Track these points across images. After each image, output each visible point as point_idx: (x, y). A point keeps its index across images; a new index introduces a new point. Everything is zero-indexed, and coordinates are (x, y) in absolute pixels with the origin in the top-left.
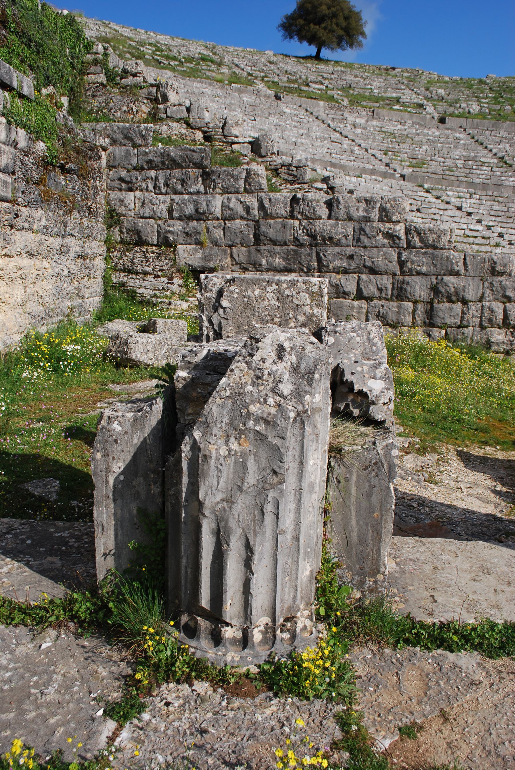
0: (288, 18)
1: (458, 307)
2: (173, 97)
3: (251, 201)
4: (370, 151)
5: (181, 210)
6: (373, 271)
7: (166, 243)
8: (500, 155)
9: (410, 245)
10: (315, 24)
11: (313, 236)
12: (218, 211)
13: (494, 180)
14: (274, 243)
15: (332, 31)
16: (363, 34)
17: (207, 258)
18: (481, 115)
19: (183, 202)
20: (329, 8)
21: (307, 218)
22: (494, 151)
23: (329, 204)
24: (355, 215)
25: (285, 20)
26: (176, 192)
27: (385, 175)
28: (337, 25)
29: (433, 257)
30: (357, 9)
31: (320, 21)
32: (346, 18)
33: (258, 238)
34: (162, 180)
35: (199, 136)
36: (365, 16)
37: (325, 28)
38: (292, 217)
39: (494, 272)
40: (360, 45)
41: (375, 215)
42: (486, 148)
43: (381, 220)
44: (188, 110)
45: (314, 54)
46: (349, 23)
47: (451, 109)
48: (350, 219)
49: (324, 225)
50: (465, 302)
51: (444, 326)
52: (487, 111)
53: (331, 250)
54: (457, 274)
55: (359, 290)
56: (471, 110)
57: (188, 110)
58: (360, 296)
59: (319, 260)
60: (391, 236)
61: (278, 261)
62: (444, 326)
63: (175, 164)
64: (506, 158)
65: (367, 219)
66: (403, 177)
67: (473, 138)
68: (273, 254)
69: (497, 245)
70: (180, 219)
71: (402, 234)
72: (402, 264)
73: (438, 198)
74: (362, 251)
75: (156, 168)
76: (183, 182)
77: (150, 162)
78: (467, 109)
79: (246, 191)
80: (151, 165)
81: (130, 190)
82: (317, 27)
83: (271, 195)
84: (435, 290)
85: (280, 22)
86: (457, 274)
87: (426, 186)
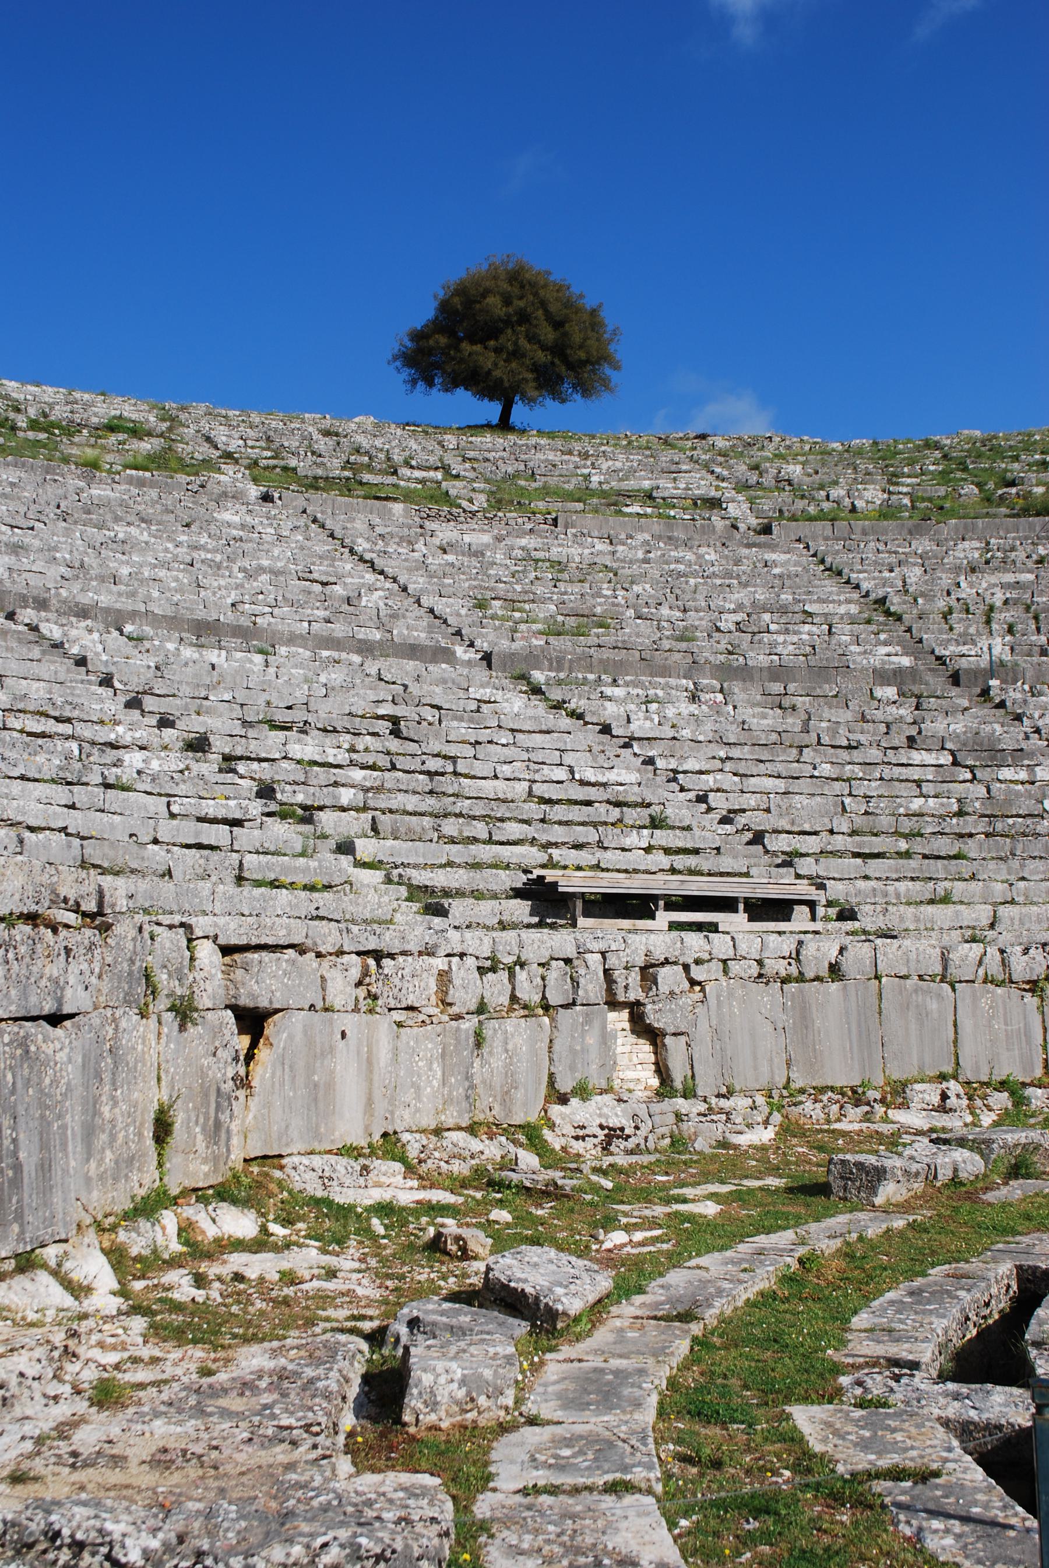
0: (418, 336)
10: (473, 342)
15: (516, 354)
18: (888, 512)
20: (507, 301)
22: (865, 586)
25: (409, 344)
28: (532, 338)
30: (589, 303)
31: (487, 332)
32: (558, 325)
36: (610, 318)
37: (497, 351)
42: (848, 582)
45: (495, 421)
46: (565, 334)
47: (800, 504)
52: (906, 501)
56: (860, 504)
67: (822, 561)
69: (656, 823)
73: (558, 706)
78: (847, 502)
82: (478, 348)
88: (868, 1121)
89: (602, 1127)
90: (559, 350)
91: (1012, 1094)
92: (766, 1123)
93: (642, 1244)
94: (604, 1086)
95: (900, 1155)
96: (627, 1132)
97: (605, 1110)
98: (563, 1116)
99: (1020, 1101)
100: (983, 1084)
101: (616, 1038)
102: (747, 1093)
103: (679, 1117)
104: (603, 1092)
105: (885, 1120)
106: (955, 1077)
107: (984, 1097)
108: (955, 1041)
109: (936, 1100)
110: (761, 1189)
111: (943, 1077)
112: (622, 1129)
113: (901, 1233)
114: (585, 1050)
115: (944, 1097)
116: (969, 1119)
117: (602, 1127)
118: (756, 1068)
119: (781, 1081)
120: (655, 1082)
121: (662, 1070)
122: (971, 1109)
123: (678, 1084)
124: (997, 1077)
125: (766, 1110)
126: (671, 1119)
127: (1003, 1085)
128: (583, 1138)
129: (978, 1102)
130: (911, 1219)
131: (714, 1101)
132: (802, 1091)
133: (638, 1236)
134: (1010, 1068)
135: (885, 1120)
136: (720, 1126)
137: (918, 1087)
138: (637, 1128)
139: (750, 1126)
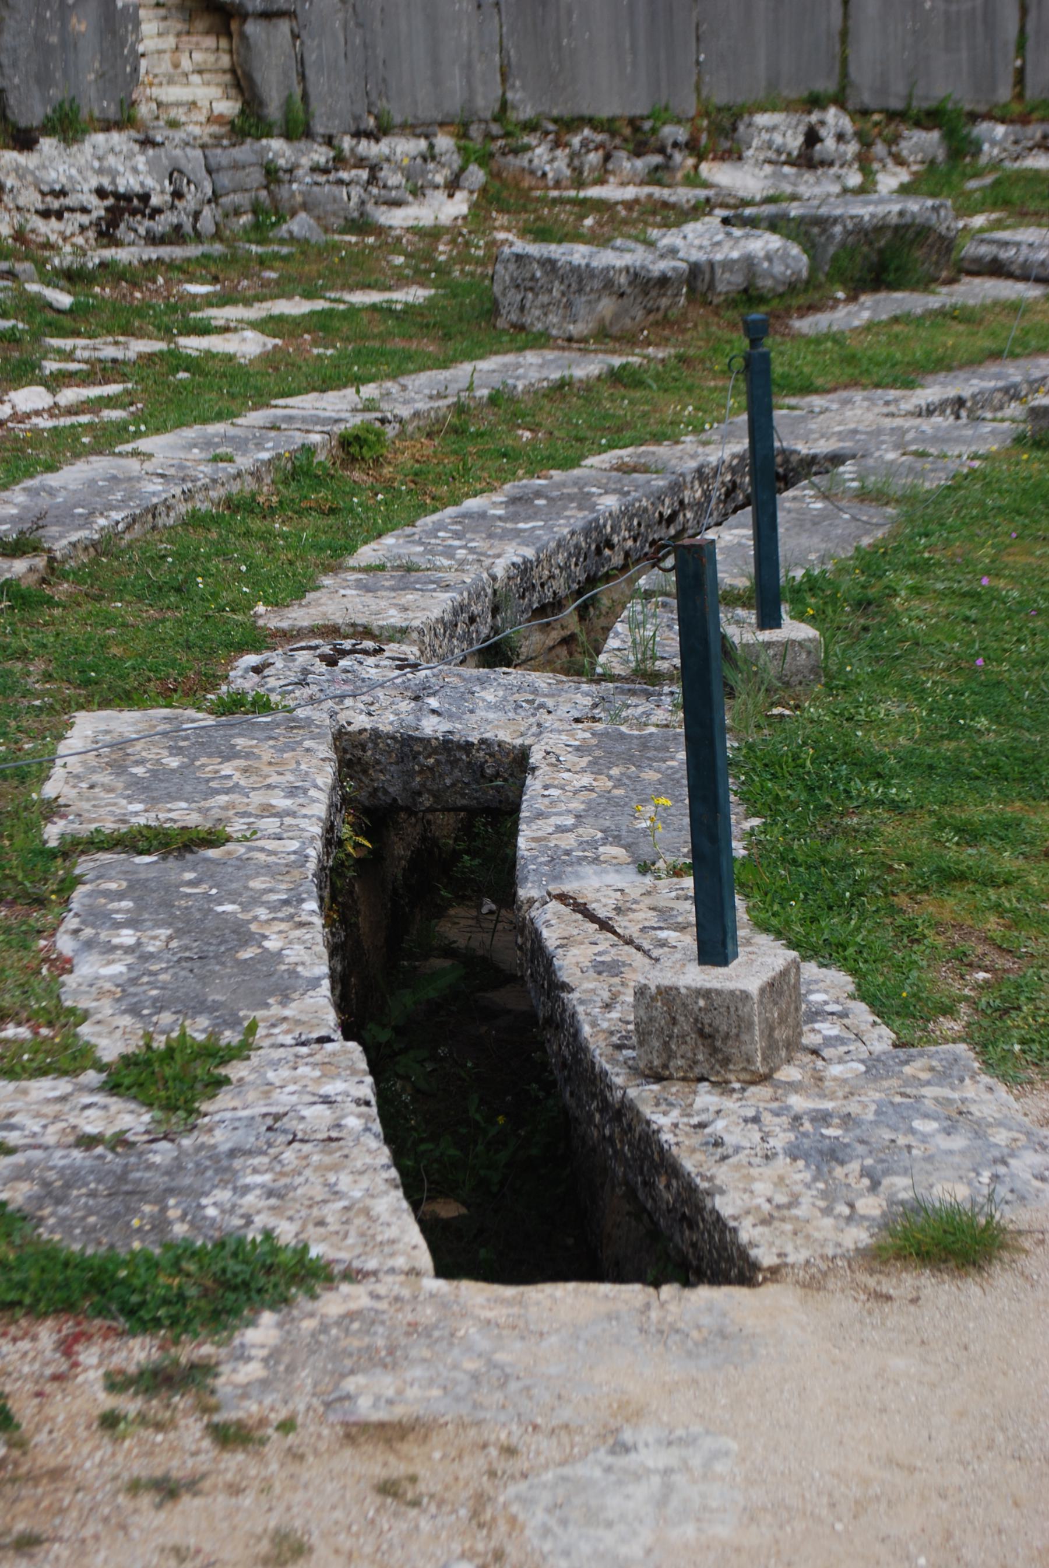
88: (659, 183)
89: (101, 193)
91: (950, 135)
92: (452, 186)
93: (72, 411)
94: (112, 111)
95: (650, 244)
96: (155, 201)
97: (111, 161)
98: (20, 172)
99: (961, 149)
100: (892, 116)
101: (137, 24)
102: (411, 129)
103: (272, 174)
104: (107, 126)
105: (693, 180)
106: (840, 101)
107: (893, 140)
108: (844, 34)
109: (795, 142)
110: (374, 308)
111: (815, 102)
112: (145, 197)
113: (588, 389)
114: (69, 43)
115: (812, 137)
116: (855, 179)
117: (101, 193)
118: (436, 81)
119: (485, 103)
120: (228, 107)
121: (242, 82)
122: (864, 162)
123: (274, 110)
124: (919, 105)
125: (456, 161)
126: (256, 177)
127: (931, 118)
128: (59, 215)
129: (879, 149)
130: (617, 361)
131: (347, 143)
132: (531, 127)
133: (69, 396)
134: (947, 85)
135: (693, 180)
136: (356, 192)
137: (762, 119)
138: (178, 195)
139: (418, 192)
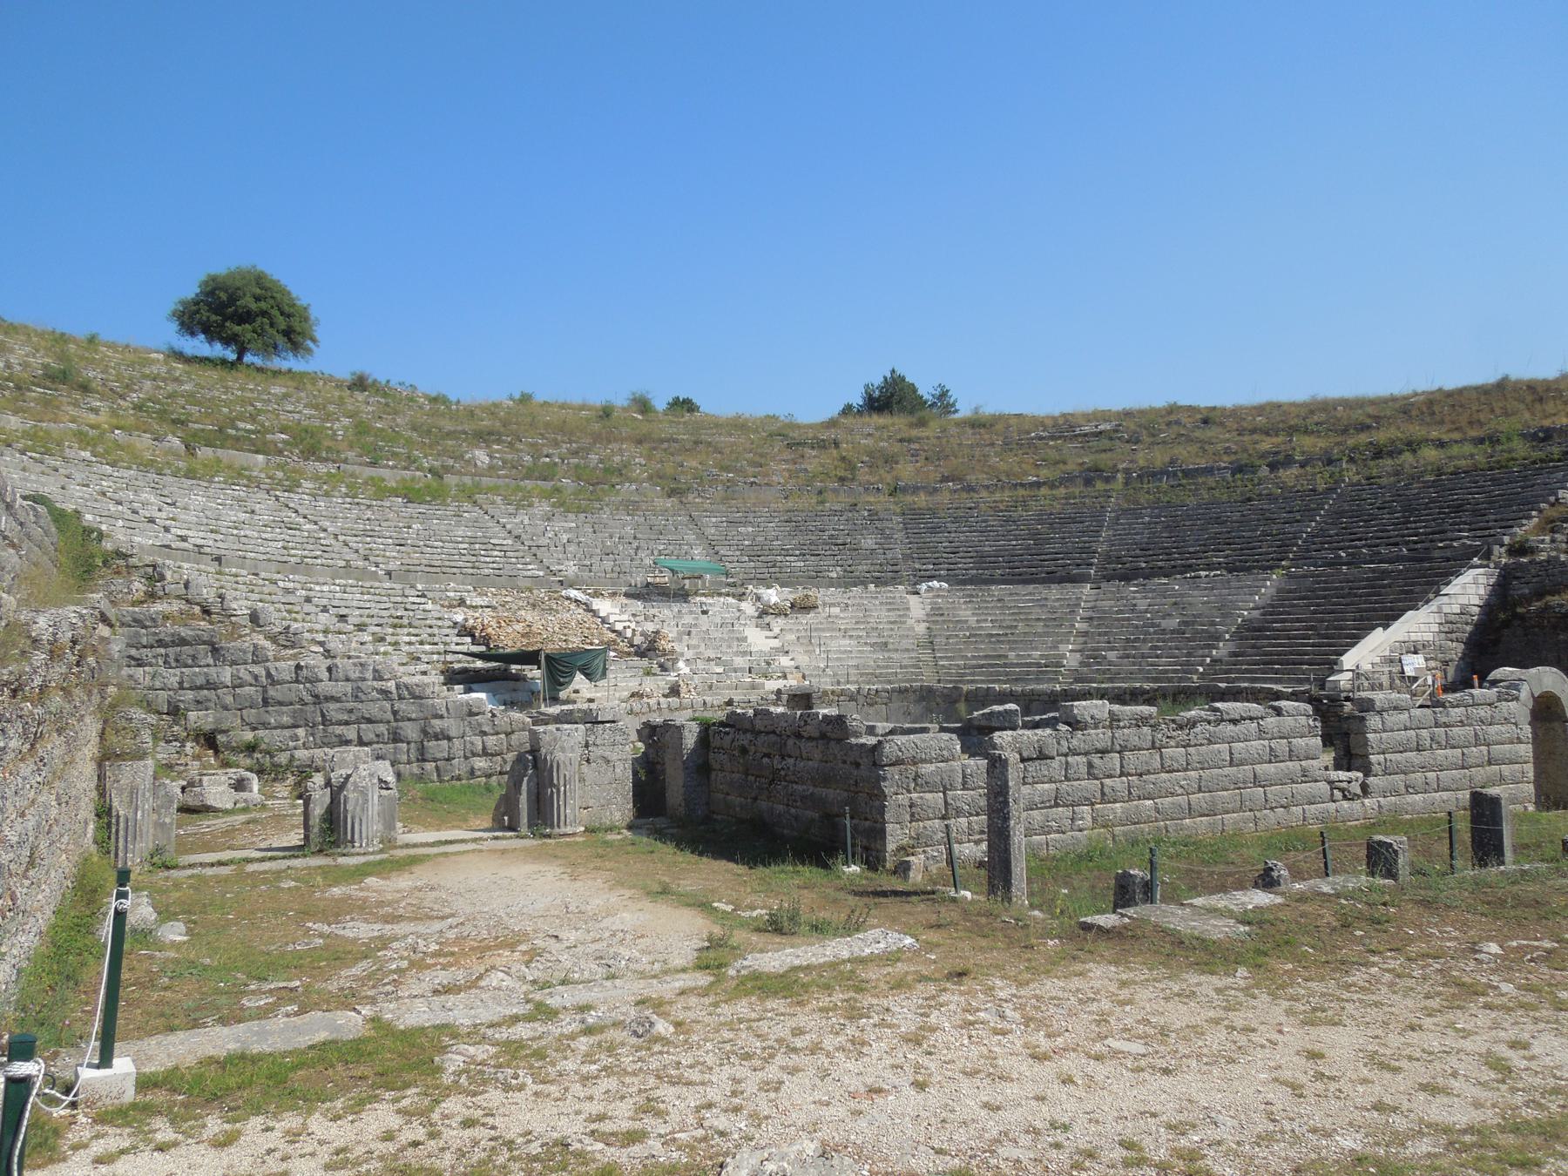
1: (445, 743)
2: (168, 575)
3: (259, 670)
4: (341, 538)
5: (192, 681)
6: (369, 721)
7: (175, 711)
8: (515, 533)
9: (401, 698)
11: (317, 696)
12: (227, 680)
13: (508, 570)
14: (281, 704)
16: (314, 340)
17: (218, 721)
19: (195, 674)
21: (311, 682)
23: (329, 669)
24: (353, 676)
26: (186, 666)
27: (363, 574)
29: (421, 705)
30: (303, 302)
31: (245, 317)
33: (266, 702)
34: (172, 657)
35: (197, 609)
36: (314, 313)
38: (297, 681)
39: (471, 714)
40: (309, 351)
41: (369, 675)
43: (374, 679)
44: (186, 586)
48: (348, 680)
49: (326, 687)
50: (449, 739)
51: (435, 760)
53: (332, 706)
54: (442, 717)
55: (360, 737)
57: (186, 586)
58: (361, 743)
59: (323, 715)
60: (385, 693)
61: (286, 719)
62: (435, 760)
63: (183, 642)
64: (524, 536)
65: (364, 679)
66: (389, 573)
68: (281, 714)
70: (191, 689)
71: (393, 689)
72: (395, 713)
74: (360, 706)
75: (166, 646)
76: (194, 657)
77: (160, 641)
79: (253, 662)
80: (161, 643)
81: (139, 666)
83: (278, 664)
84: (424, 732)
85: (173, 307)
86: (442, 717)
87: (419, 587)
90: (288, 333)
